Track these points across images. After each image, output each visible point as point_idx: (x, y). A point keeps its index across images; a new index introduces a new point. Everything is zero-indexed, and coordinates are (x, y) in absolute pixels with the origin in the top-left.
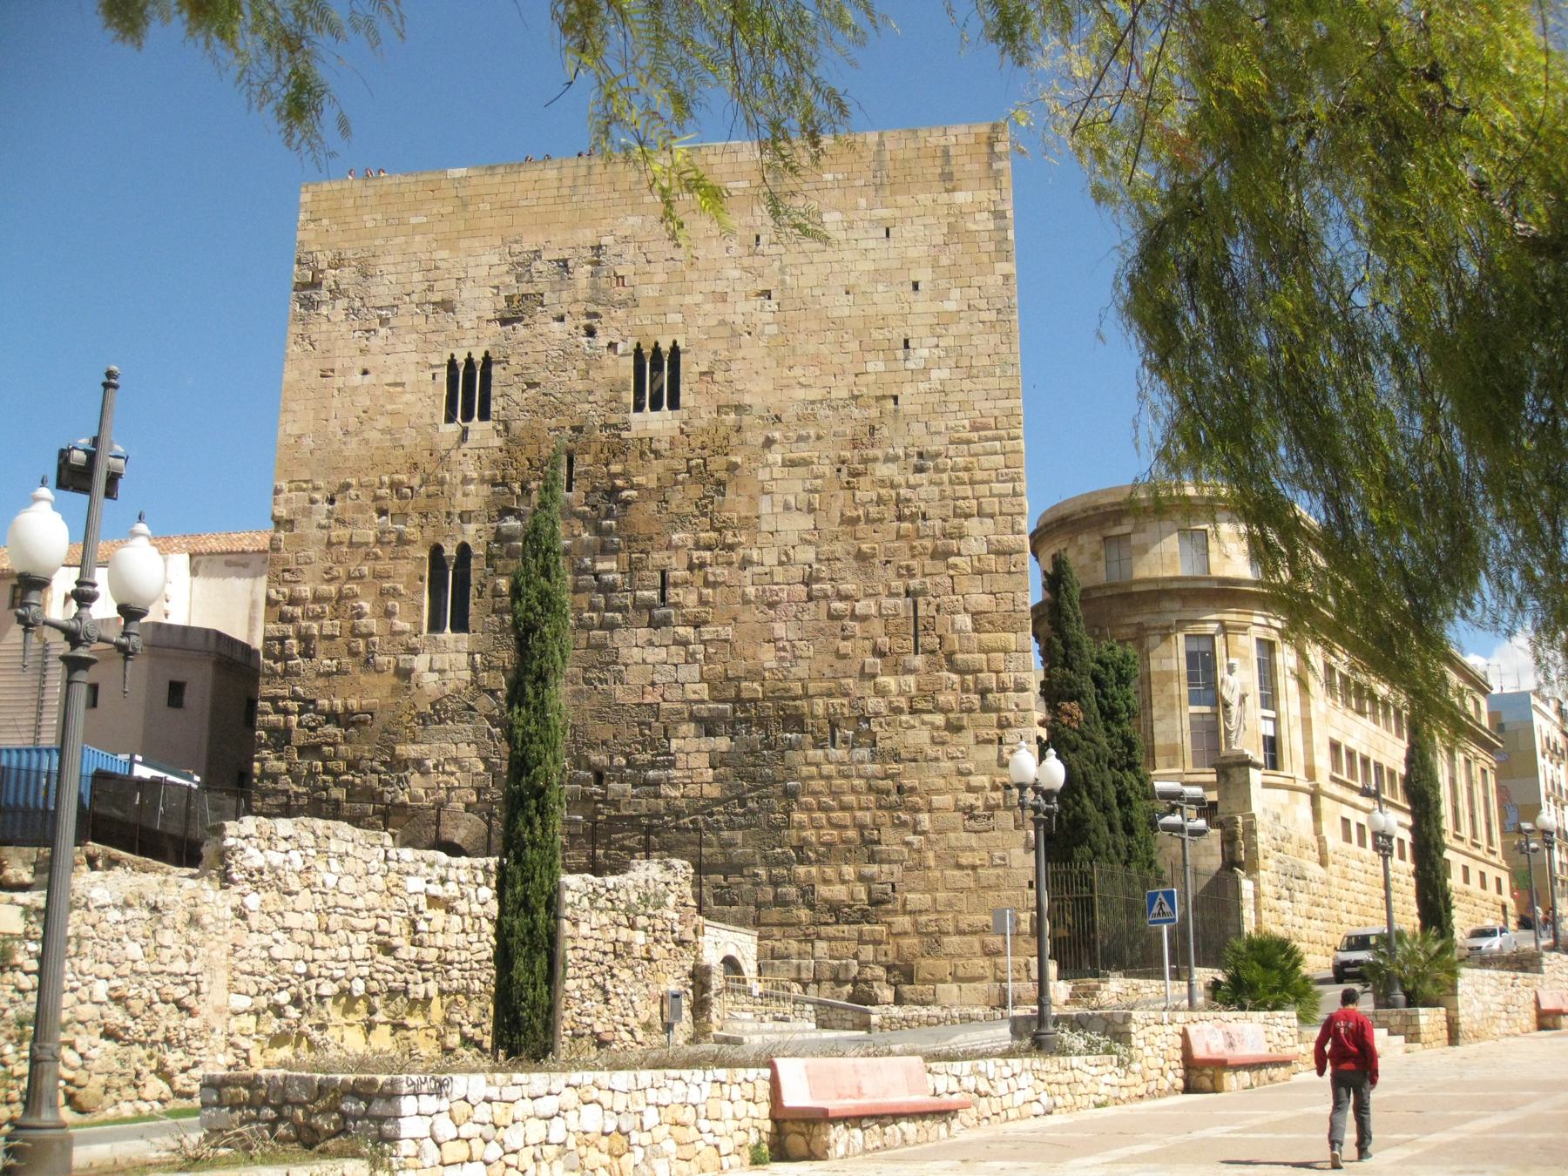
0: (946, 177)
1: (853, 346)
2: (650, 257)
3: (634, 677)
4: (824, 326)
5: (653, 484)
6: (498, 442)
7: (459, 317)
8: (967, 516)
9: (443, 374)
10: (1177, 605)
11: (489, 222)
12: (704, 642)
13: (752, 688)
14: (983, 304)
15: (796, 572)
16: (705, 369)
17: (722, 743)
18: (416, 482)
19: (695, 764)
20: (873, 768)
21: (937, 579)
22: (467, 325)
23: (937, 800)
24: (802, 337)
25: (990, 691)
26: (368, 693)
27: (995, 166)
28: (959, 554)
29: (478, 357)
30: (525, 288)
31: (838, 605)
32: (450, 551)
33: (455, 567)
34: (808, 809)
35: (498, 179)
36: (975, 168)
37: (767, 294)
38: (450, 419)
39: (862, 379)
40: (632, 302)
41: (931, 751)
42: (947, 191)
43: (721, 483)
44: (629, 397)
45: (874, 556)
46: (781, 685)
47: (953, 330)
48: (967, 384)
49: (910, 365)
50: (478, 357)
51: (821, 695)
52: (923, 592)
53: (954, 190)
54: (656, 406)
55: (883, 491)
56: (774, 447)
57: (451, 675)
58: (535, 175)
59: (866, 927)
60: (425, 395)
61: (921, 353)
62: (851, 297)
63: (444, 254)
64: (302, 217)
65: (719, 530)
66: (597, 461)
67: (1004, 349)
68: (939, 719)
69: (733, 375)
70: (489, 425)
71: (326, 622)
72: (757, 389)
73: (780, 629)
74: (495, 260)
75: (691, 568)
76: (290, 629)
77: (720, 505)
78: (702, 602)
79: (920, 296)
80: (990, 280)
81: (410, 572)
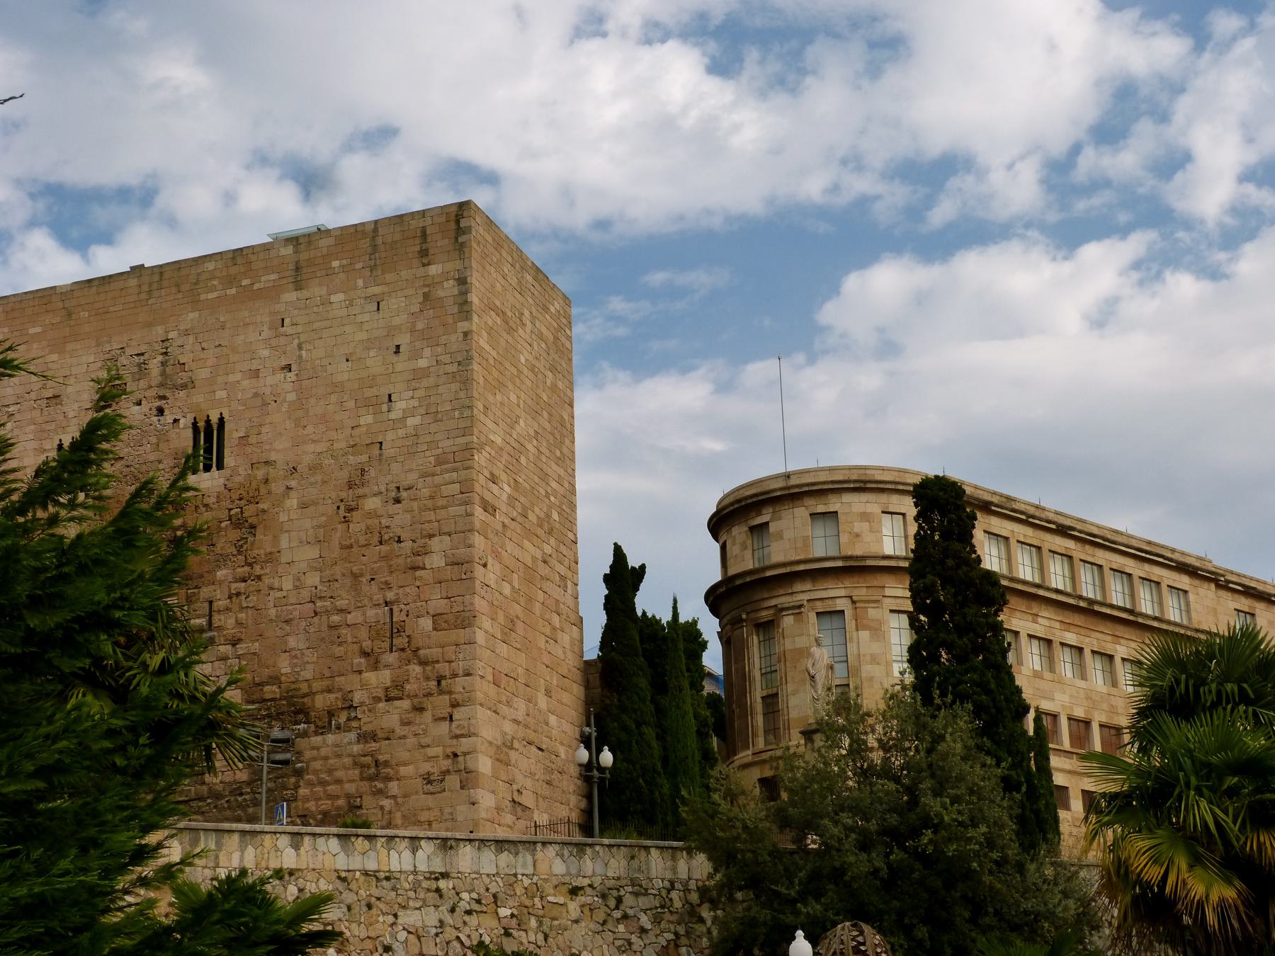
0: (424, 253)
1: (351, 404)
2: (204, 345)
4: (329, 390)
7: (65, 409)
8: (431, 536)
10: (808, 586)
12: (238, 657)
13: (271, 691)
14: (447, 359)
15: (306, 594)
16: (242, 434)
20: (356, 749)
21: (407, 589)
22: (71, 414)
23: (403, 770)
24: (313, 401)
25: (444, 677)
27: (460, 240)
28: (424, 568)
31: (336, 618)
34: (310, 784)
35: (94, 290)
36: (445, 243)
37: (288, 368)
39: (356, 432)
41: (400, 731)
42: (424, 265)
43: (253, 527)
45: (362, 575)
46: (293, 686)
47: (425, 383)
48: (433, 427)
49: (393, 416)
51: (322, 692)
52: (397, 601)
53: (429, 264)
55: (369, 522)
56: (292, 494)
61: (400, 406)
62: (350, 364)
63: (54, 357)
65: (251, 565)
68: (406, 704)
69: (264, 438)
72: (281, 447)
73: (292, 642)
74: (92, 359)
75: (230, 597)
77: (253, 543)
78: (239, 623)
79: (402, 356)
80: (453, 338)
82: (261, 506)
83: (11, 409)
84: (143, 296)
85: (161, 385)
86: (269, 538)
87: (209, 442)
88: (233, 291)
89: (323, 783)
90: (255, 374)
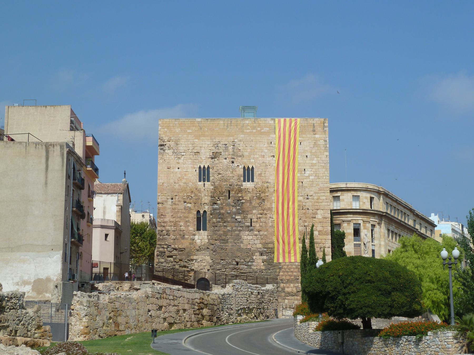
0: (314, 131)
3: (245, 242)
5: (248, 199)
6: (212, 187)
8: (317, 210)
9: (198, 169)
11: (207, 133)
12: (260, 235)
14: (321, 162)
17: (265, 257)
18: (193, 195)
19: (259, 262)
26: (184, 244)
29: (206, 167)
30: (217, 151)
32: (202, 212)
33: (203, 216)
34: (283, 272)
38: (200, 181)
40: (242, 156)
44: (242, 179)
47: (315, 167)
48: (318, 180)
49: (305, 175)
50: (206, 167)
54: (248, 181)
57: (203, 241)
58: (218, 122)
59: (296, 297)
60: (194, 175)
61: (307, 173)
63: (197, 140)
64: (160, 127)
65: (263, 210)
66: (235, 193)
67: (326, 172)
70: (209, 183)
71: (172, 227)
76: (163, 228)
77: (264, 204)
78: (260, 226)
80: (323, 156)
81: (193, 216)
82: (266, 194)
83: (182, 154)
84: (225, 127)
85: (233, 155)
86: (269, 203)
87: (249, 174)
88: (255, 131)
89: (287, 272)
90: (263, 156)
